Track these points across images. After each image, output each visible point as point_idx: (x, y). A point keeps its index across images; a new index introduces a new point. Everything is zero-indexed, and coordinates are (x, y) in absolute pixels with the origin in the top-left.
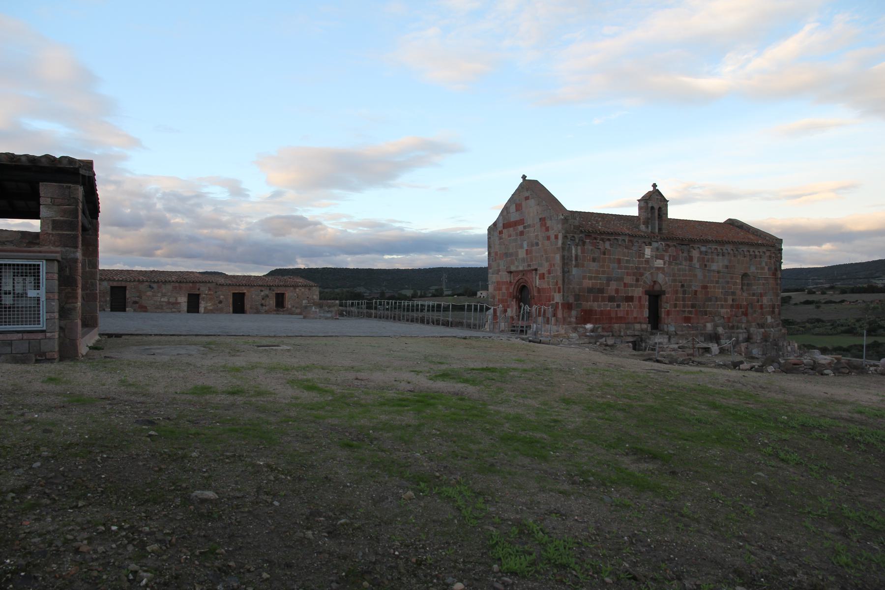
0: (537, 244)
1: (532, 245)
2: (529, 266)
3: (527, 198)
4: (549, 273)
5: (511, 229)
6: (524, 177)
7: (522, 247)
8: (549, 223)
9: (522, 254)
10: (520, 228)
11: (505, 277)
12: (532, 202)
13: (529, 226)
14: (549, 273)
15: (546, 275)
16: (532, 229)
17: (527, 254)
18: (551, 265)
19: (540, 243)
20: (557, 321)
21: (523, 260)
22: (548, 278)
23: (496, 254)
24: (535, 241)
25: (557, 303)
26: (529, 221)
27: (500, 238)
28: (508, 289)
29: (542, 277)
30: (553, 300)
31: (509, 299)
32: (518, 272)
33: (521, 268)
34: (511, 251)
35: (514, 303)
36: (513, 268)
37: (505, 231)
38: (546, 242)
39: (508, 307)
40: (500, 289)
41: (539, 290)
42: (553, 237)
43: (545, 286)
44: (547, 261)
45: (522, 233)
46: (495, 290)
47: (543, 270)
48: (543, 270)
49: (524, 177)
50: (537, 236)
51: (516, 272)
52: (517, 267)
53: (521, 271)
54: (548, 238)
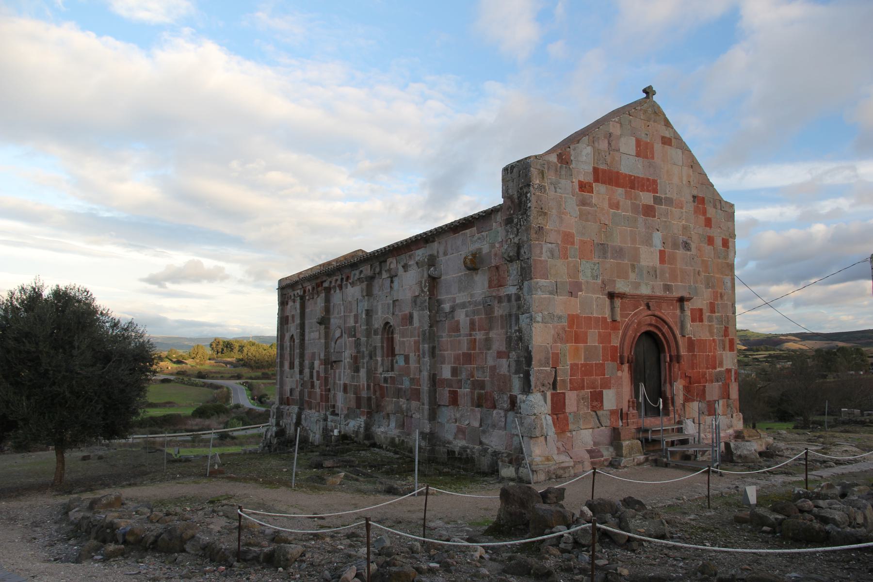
0: (687, 246)
1: (675, 246)
2: (667, 288)
3: (666, 141)
4: (713, 311)
5: (620, 190)
6: (648, 92)
7: (648, 242)
8: (711, 212)
9: (649, 258)
10: (646, 198)
11: (597, 306)
12: (674, 153)
13: (669, 201)
14: (713, 311)
15: (706, 314)
16: (676, 211)
17: (662, 260)
18: (715, 294)
19: (693, 246)
20: (728, 406)
21: (653, 273)
22: (710, 319)
23: (568, 238)
24: (682, 238)
25: (728, 371)
26: (667, 190)
27: (583, 203)
28: (604, 339)
29: (698, 315)
30: (721, 365)
31: (610, 366)
32: (636, 299)
33: (645, 290)
34: (617, 242)
35: (624, 374)
36: (621, 287)
37: (600, 189)
38: (708, 249)
39: (606, 385)
40: (578, 338)
41: (691, 344)
42: (718, 242)
43: (705, 335)
44: (708, 286)
45: (649, 211)
46: (558, 338)
47: (700, 302)
48: (700, 302)
49: (648, 92)
50: (685, 228)
51: (634, 297)
52: (637, 285)
53: (650, 297)
54: (710, 241)
